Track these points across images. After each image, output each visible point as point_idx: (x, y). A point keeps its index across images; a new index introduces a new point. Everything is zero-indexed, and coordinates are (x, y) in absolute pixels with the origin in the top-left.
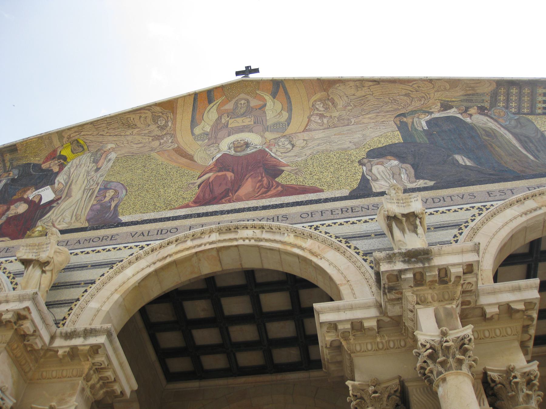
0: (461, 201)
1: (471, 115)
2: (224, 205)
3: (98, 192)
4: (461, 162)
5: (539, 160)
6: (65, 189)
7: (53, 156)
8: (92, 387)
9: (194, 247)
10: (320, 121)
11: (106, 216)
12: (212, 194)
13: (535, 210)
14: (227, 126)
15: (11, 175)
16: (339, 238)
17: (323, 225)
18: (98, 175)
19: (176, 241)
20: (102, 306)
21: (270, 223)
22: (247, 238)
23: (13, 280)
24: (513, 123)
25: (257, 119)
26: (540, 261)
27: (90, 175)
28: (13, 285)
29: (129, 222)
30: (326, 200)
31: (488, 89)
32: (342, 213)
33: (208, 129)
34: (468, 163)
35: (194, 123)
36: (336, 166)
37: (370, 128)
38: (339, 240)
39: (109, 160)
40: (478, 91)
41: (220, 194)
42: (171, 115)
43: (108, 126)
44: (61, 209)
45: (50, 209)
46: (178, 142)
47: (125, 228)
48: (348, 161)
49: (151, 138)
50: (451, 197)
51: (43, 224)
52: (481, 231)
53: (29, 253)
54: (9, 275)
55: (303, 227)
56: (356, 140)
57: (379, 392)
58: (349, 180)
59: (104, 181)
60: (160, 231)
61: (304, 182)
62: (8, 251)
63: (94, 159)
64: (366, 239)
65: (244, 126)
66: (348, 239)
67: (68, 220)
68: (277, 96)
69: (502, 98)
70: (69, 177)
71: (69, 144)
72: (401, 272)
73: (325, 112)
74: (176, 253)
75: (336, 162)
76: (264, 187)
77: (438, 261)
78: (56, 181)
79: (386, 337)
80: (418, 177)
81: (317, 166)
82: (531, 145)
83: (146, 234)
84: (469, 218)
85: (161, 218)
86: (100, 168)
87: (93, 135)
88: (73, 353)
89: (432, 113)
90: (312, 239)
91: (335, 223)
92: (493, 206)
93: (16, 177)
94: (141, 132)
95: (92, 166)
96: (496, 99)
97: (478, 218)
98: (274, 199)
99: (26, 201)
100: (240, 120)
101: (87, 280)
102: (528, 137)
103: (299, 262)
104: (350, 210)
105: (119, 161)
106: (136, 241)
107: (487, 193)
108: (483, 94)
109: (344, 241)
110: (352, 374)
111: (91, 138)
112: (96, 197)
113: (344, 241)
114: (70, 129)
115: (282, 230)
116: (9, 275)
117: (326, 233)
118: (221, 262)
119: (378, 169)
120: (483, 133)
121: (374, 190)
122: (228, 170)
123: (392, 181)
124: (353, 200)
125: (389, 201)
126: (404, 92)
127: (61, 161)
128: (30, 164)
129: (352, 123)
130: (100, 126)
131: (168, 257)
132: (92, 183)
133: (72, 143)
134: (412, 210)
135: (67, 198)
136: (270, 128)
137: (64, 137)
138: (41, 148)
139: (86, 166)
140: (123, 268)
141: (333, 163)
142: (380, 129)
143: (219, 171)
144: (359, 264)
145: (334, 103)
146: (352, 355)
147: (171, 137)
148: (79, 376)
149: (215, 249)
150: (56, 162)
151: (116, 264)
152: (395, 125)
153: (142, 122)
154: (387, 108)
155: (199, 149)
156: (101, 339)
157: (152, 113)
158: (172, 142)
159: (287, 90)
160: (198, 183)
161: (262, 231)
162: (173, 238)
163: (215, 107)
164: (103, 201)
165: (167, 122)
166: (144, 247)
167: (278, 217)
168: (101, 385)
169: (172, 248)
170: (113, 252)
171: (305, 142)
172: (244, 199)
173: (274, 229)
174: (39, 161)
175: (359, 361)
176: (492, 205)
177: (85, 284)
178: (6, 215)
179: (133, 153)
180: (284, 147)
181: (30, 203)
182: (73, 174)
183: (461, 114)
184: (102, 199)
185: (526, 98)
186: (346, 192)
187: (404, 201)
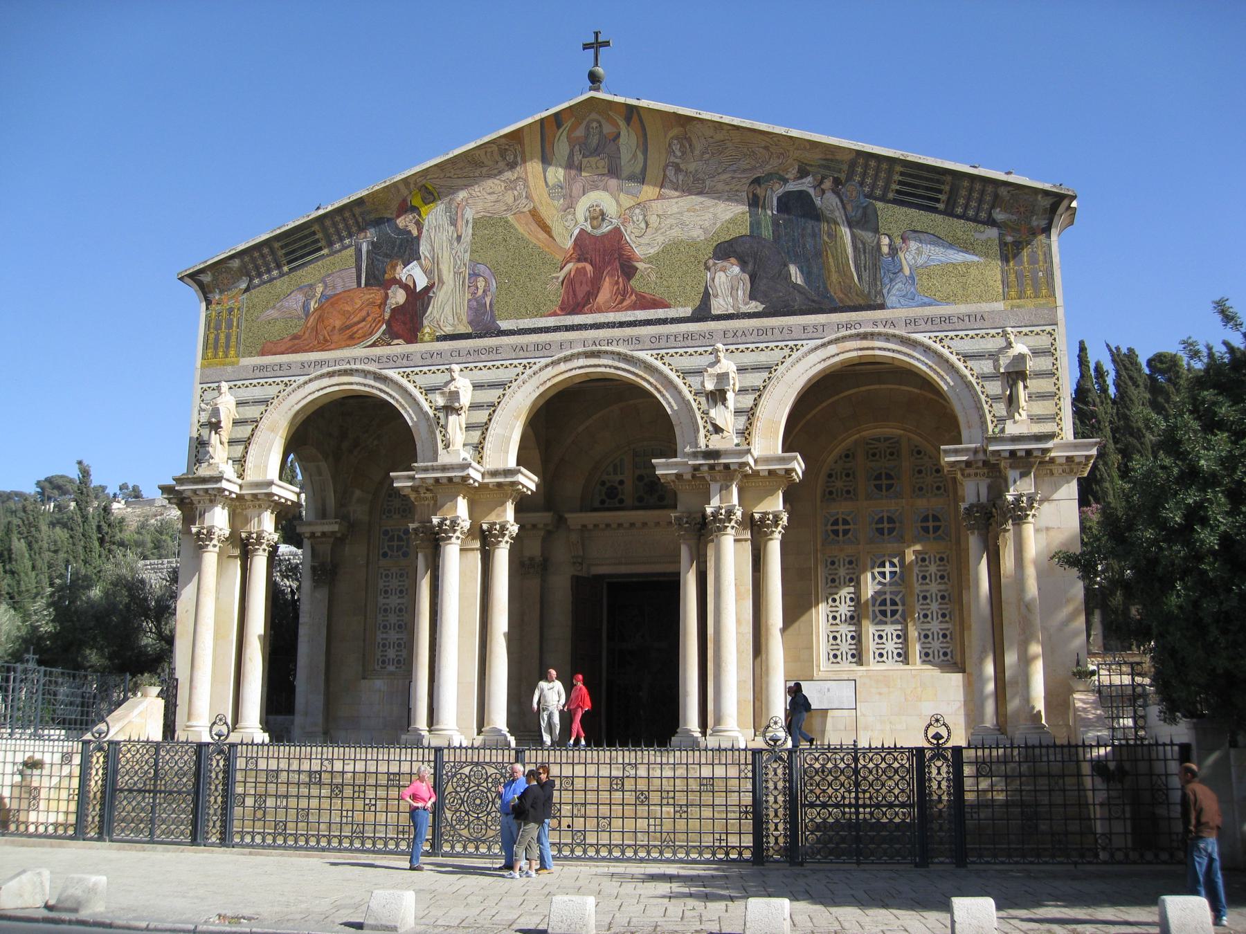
4: (793, 279)
15: (368, 235)
24: (860, 211)
31: (848, 157)
34: (799, 282)
39: (467, 221)
40: (838, 157)
42: (518, 147)
46: (533, 201)
47: (505, 338)
56: (707, 224)
68: (632, 123)
69: (859, 170)
80: (752, 297)
82: (863, 257)
88: (499, 485)
89: (786, 181)
98: (629, 312)
100: (593, 160)
102: (864, 244)
108: (841, 162)
122: (586, 260)
126: (763, 144)
143: (579, 260)
154: (744, 164)
158: (527, 197)
160: (561, 279)
165: (515, 157)
169: (550, 372)
170: (502, 369)
181: (405, 287)
185: (883, 175)
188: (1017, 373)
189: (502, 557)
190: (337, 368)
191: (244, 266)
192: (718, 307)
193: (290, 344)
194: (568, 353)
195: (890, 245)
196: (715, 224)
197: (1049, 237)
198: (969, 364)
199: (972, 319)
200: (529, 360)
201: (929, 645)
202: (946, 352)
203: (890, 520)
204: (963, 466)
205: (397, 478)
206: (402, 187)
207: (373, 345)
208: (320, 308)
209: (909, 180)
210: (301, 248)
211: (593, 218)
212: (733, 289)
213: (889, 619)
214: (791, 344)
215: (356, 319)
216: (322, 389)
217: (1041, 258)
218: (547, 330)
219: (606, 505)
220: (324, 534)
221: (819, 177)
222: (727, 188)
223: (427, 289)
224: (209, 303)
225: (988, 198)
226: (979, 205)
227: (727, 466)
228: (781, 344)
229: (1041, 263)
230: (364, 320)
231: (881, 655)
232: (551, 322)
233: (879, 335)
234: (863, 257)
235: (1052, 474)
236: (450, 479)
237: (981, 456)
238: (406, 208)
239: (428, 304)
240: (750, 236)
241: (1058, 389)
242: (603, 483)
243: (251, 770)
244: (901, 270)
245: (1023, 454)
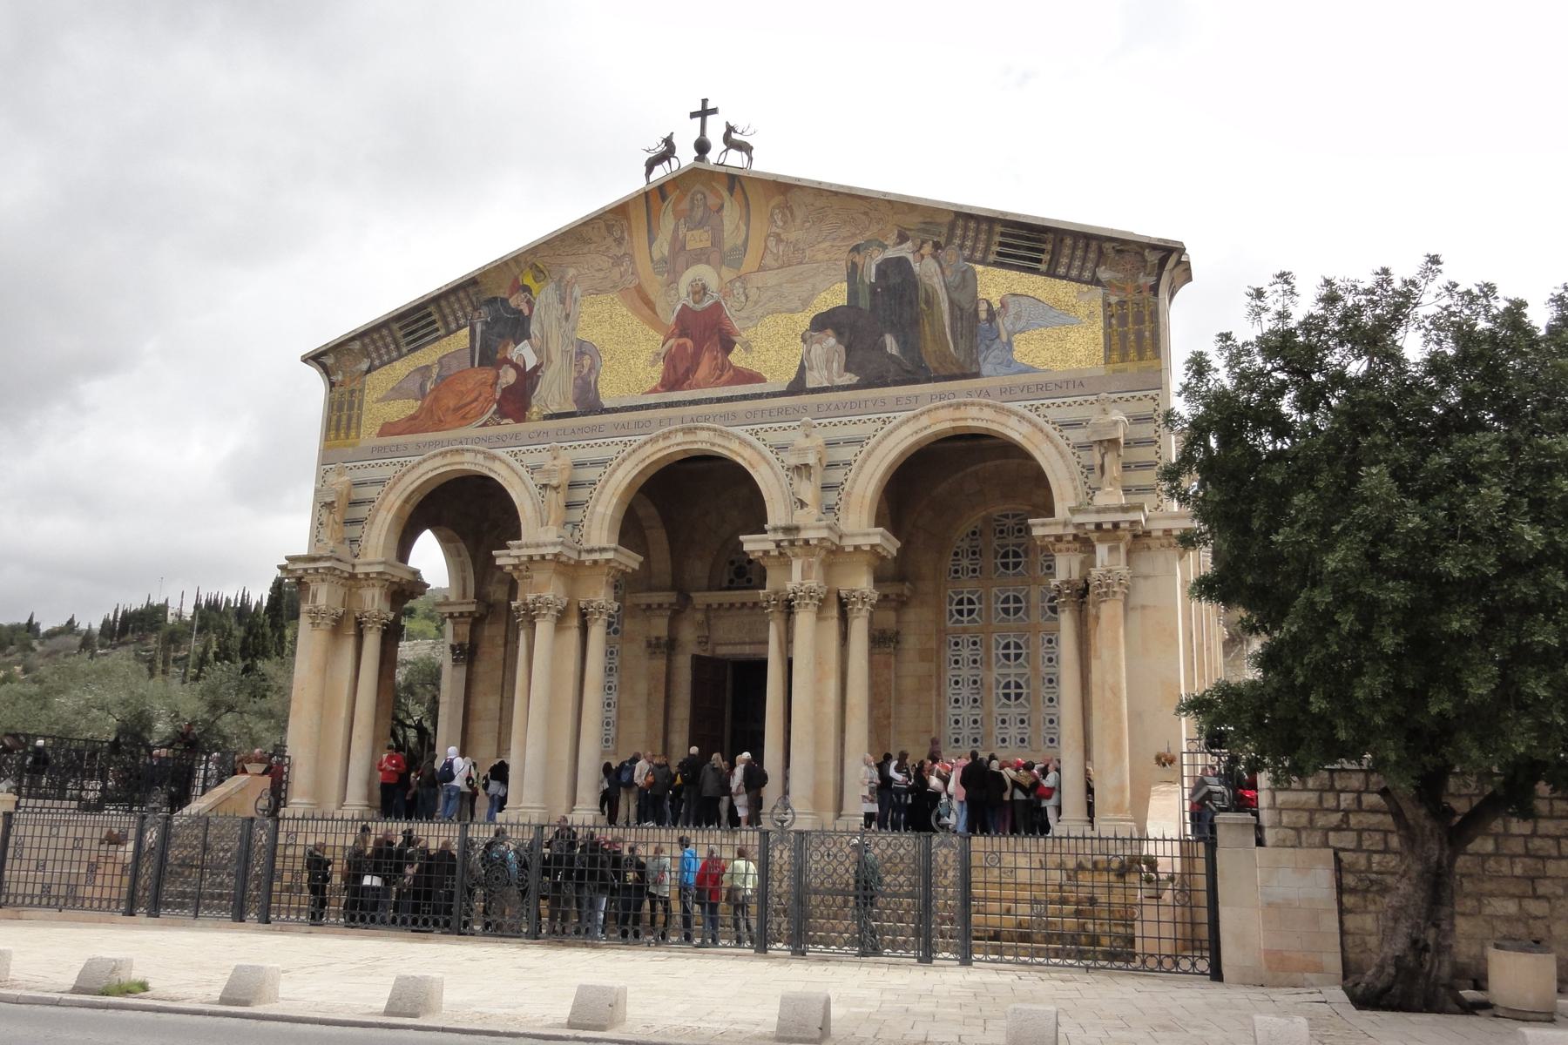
4: (888, 349)
10: (775, 251)
13: (925, 428)
14: (683, 247)
31: (948, 219)
34: (894, 352)
35: (651, 242)
42: (625, 222)
65: (701, 249)
69: (959, 232)
72: (781, 541)
74: (653, 454)
77: (804, 535)
80: (847, 369)
82: (959, 325)
88: (595, 562)
89: (884, 247)
98: (726, 388)
102: (961, 310)
108: (939, 224)
120: (923, 296)
143: (681, 336)
145: (792, 214)
160: (663, 355)
165: (622, 232)
169: (649, 449)
181: (515, 366)
183: (914, 253)
188: (1109, 441)
189: (597, 633)
190: (450, 447)
191: (364, 346)
192: (812, 380)
194: (666, 430)
195: (988, 310)
196: (813, 295)
197: (1156, 294)
198: (1066, 433)
199: (1071, 385)
200: (630, 438)
201: (1053, 731)
202: (1041, 421)
203: (1017, 600)
204: (1052, 539)
205: (499, 556)
206: (512, 265)
207: (485, 425)
208: (437, 388)
209: (1010, 240)
211: (695, 293)
212: (828, 362)
213: (1012, 702)
214: (883, 416)
215: (469, 399)
217: (1147, 318)
218: (648, 407)
219: (735, 585)
220: (461, 614)
221: (918, 242)
222: (826, 257)
223: (536, 368)
224: (332, 385)
225: (1092, 255)
226: (1083, 264)
227: (807, 542)
228: (874, 417)
229: (1147, 324)
230: (476, 400)
231: (1004, 740)
232: (652, 399)
233: (973, 404)
234: (959, 325)
235: (1149, 548)
236: (543, 557)
237: (1071, 530)
239: (537, 383)
240: (848, 306)
241: (1160, 458)
242: (732, 563)
243: (291, 844)
244: (998, 336)
245: (1109, 526)
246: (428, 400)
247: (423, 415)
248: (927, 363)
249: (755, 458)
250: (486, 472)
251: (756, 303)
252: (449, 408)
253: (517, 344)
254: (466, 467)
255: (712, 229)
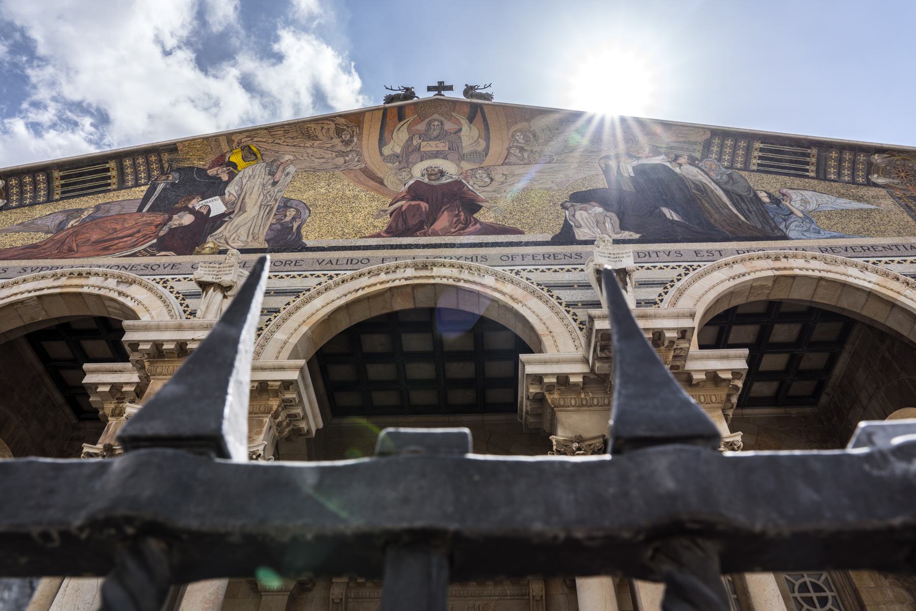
0: (667, 258)
1: (680, 165)
2: (419, 238)
3: (277, 210)
4: (668, 217)
5: (750, 222)
6: (237, 202)
7: (221, 161)
8: (279, 425)
9: (388, 282)
10: (520, 155)
11: (288, 238)
12: (405, 224)
14: (419, 150)
15: (170, 178)
16: (541, 286)
17: (524, 270)
18: (276, 190)
19: (369, 273)
20: (289, 338)
21: (469, 262)
22: (445, 277)
23: (182, 302)
24: (725, 178)
25: (452, 145)
26: (735, 324)
27: (266, 188)
28: (183, 307)
29: (315, 247)
30: (527, 244)
31: (703, 137)
32: (544, 259)
33: (398, 150)
35: (382, 142)
36: (538, 208)
37: (574, 168)
38: (541, 287)
39: (288, 174)
41: (414, 226)
42: (357, 130)
43: (285, 134)
44: (234, 225)
45: (221, 223)
46: (364, 161)
47: (310, 253)
48: (550, 203)
49: (334, 154)
50: (656, 252)
51: (214, 241)
52: (687, 292)
53: (209, 274)
54: (177, 295)
55: (504, 270)
57: (583, 449)
58: (551, 225)
59: (282, 197)
60: (350, 261)
61: (503, 222)
62: (173, 268)
63: (270, 171)
64: (569, 289)
65: (438, 151)
66: (550, 287)
67: (243, 237)
69: (715, 149)
70: (242, 189)
71: (240, 149)
73: (525, 145)
74: (369, 286)
75: (537, 203)
76: (462, 223)
78: (226, 191)
79: (590, 394)
80: (623, 227)
81: (517, 205)
82: (743, 204)
83: (334, 263)
84: (675, 277)
85: (351, 246)
86: (277, 182)
87: (268, 143)
89: (639, 158)
90: (513, 284)
91: (536, 270)
92: (700, 267)
93: (177, 182)
94: (322, 145)
95: (268, 178)
96: (708, 150)
97: (685, 279)
98: (473, 237)
99: (192, 211)
100: (433, 143)
101: (271, 308)
102: (740, 196)
103: (499, 307)
104: (552, 257)
105: (299, 176)
106: (324, 269)
107: (694, 253)
109: (546, 289)
110: (551, 427)
111: (265, 146)
112: (275, 215)
113: (546, 289)
114: (241, 132)
115: (482, 272)
116: (177, 295)
117: (527, 279)
118: (414, 299)
119: (581, 215)
120: (693, 186)
121: (577, 238)
123: (596, 229)
124: (555, 247)
125: (600, 254)
127: (230, 169)
128: (194, 168)
129: (554, 161)
130: (276, 133)
131: (361, 290)
132: (269, 199)
133: (244, 148)
134: (623, 267)
135: (242, 212)
136: (467, 157)
137: (234, 141)
138: (206, 151)
139: (260, 178)
140: (311, 298)
141: (534, 204)
142: (584, 170)
143: (413, 199)
144: (561, 315)
146: (555, 409)
147: (357, 155)
148: (267, 413)
149: (410, 286)
150: (225, 169)
151: (303, 293)
152: (600, 168)
153: (324, 134)
155: (389, 173)
156: (294, 375)
157: (336, 124)
158: (358, 161)
159: (485, 116)
160: (390, 211)
161: (461, 271)
162: (366, 269)
163: (406, 126)
164: (283, 221)
165: (352, 137)
166: (333, 277)
167: (477, 257)
168: (287, 423)
169: (365, 281)
171: (504, 177)
172: (440, 234)
173: (473, 270)
174: (204, 165)
175: (561, 416)
176: (699, 266)
177: (268, 312)
178: (168, 226)
179: (314, 169)
180: (482, 180)
182: (246, 185)
183: (671, 162)
184: (283, 218)
186: (548, 237)
187: (616, 256)
193: (22, 252)
209: (770, 155)
210: (84, 182)
215: (120, 235)
216: (35, 291)
223: (223, 215)
230: (131, 235)
238: (221, 161)
246: (64, 233)
247: (47, 246)
248: (720, 228)
249: (518, 292)
250: (115, 295)
251: (502, 183)
252: (90, 240)
253: (203, 199)
254: (85, 290)
255: (449, 141)
